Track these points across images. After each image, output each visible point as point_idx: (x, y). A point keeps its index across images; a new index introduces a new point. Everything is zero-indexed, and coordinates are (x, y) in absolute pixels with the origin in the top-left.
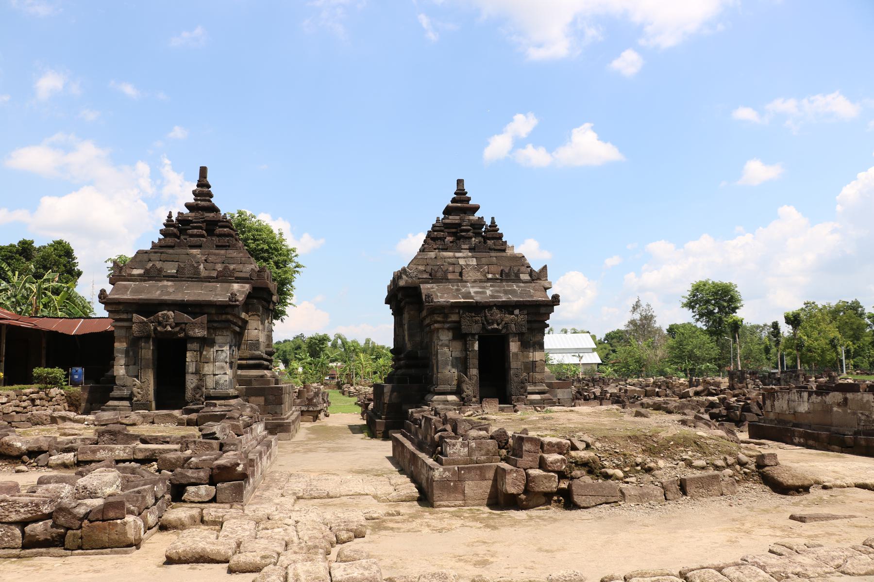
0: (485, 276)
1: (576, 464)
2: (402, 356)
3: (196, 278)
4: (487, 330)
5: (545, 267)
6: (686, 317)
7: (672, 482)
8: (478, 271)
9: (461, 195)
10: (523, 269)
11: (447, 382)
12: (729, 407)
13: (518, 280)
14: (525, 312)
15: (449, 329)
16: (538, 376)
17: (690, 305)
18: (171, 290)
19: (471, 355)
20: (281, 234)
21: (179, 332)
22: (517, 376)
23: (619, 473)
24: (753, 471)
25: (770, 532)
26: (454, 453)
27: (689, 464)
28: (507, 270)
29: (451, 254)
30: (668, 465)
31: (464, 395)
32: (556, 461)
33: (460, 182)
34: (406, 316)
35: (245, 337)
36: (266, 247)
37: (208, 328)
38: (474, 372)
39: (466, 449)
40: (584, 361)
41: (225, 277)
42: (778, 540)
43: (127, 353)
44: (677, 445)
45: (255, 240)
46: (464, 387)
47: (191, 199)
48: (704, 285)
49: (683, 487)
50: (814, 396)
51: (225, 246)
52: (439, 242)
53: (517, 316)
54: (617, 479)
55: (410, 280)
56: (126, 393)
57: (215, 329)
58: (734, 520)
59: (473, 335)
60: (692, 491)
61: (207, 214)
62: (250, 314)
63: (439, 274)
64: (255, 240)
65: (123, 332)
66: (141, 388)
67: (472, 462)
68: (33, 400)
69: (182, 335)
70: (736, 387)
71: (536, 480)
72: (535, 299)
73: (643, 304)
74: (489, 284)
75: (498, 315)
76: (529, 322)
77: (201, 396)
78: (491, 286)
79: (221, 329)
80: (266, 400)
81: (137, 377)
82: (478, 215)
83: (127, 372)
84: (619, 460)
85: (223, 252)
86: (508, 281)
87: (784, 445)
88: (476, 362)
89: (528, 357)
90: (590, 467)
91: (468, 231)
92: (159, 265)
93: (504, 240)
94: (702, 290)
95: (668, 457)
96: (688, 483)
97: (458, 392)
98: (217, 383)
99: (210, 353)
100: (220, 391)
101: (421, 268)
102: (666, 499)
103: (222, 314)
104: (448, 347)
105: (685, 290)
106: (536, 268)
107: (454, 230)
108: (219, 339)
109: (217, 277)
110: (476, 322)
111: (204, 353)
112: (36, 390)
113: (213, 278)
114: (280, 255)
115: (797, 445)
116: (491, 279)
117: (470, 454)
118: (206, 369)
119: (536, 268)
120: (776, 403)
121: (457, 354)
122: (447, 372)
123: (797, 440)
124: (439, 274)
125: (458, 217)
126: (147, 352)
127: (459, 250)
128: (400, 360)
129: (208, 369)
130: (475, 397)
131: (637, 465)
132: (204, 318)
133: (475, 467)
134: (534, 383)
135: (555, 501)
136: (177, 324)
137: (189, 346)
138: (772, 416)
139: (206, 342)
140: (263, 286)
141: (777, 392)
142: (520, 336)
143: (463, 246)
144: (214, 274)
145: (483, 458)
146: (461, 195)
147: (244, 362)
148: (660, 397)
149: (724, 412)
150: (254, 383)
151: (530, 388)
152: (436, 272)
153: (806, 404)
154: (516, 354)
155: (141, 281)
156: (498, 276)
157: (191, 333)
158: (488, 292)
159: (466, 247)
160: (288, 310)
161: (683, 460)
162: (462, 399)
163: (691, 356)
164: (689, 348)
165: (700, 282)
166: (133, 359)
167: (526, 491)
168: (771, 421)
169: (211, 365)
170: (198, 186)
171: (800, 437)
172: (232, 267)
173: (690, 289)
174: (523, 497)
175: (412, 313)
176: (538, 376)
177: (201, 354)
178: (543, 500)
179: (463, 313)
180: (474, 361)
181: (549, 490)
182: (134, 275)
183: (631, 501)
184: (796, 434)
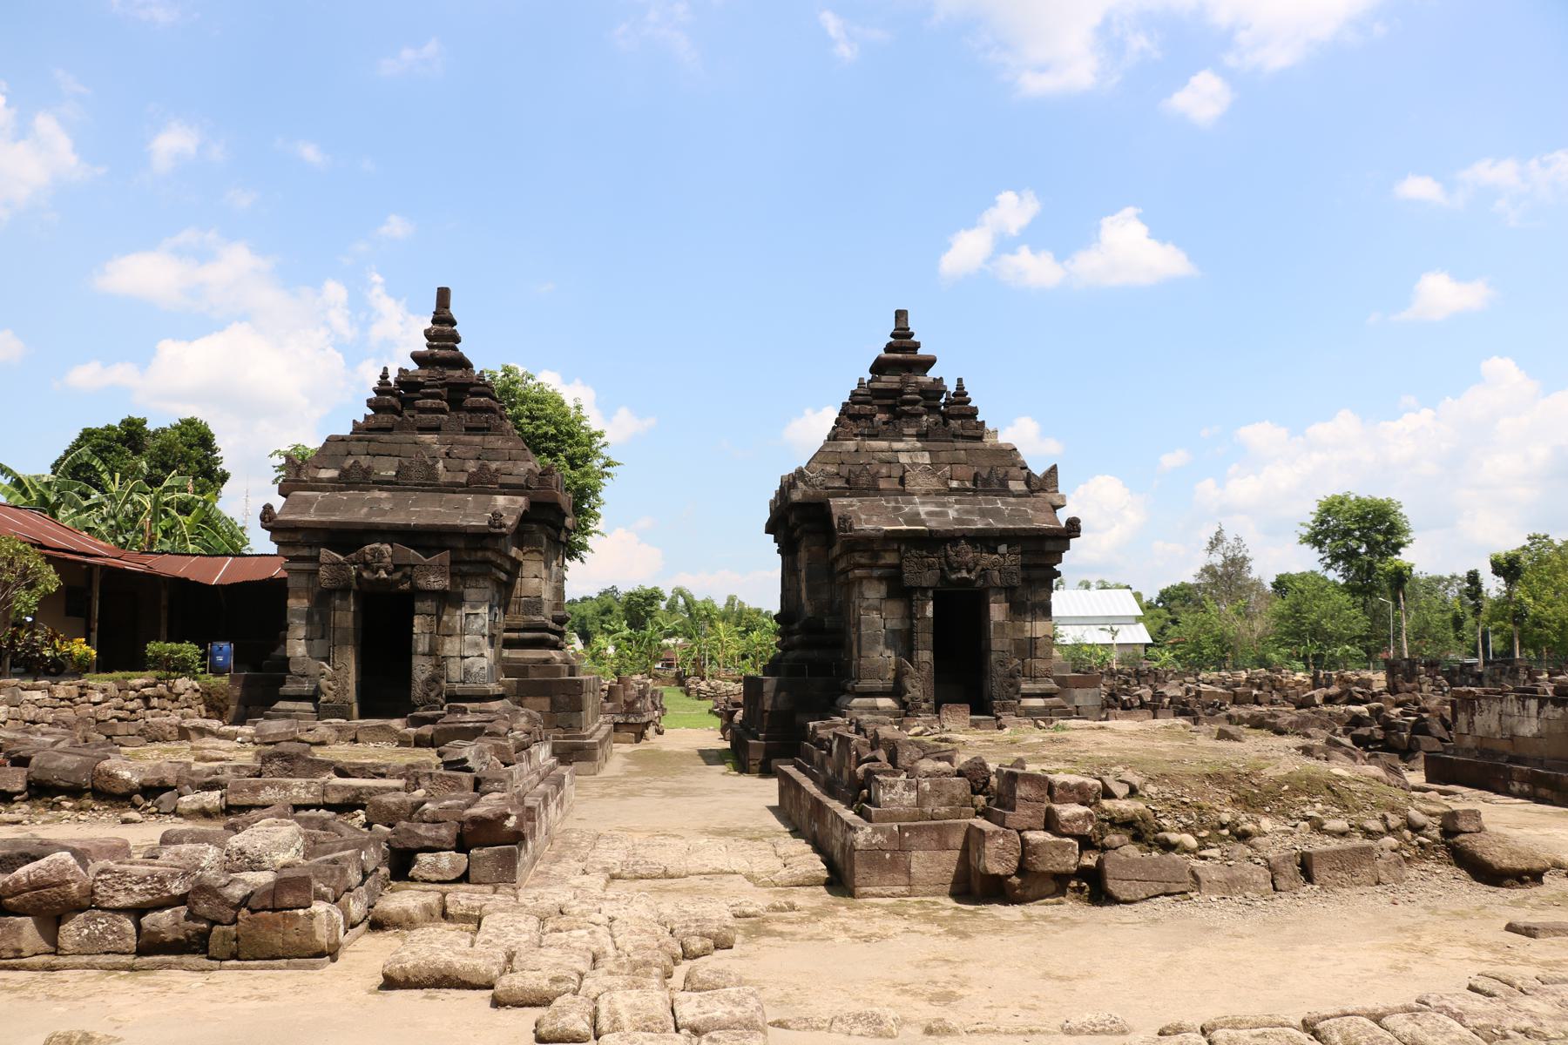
1: (1112, 822)
2: (796, 626)
3: (431, 485)
4: (951, 583)
5: (1054, 468)
6: (1307, 561)
7: (1287, 859)
8: (934, 474)
9: (902, 338)
10: (1014, 471)
11: (875, 673)
12: (1388, 725)
13: (1004, 491)
14: (1019, 549)
15: (880, 579)
16: (1040, 665)
17: (1315, 539)
18: (387, 507)
19: (919, 625)
20: (578, 408)
21: (400, 581)
22: (1002, 663)
23: (1190, 840)
24: (1436, 841)
25: (1468, 952)
26: (893, 800)
27: (1318, 827)
28: (985, 474)
29: (884, 444)
30: (1279, 827)
31: (907, 698)
32: (1076, 818)
33: (901, 315)
34: (803, 555)
35: (517, 592)
36: (552, 430)
37: (452, 575)
38: (925, 656)
39: (914, 794)
40: (1120, 639)
41: (482, 484)
42: (1485, 968)
43: (309, 617)
44: (1295, 791)
45: (533, 418)
46: (908, 683)
47: (422, 345)
48: (1342, 503)
49: (1306, 868)
50: (1550, 707)
51: (483, 429)
52: (863, 423)
53: (1003, 555)
54: (1187, 852)
55: (810, 491)
56: (307, 687)
57: (464, 576)
58: (1400, 929)
59: (924, 590)
60: (1323, 875)
61: (449, 373)
62: (526, 549)
63: (863, 481)
64: (533, 418)
65: (302, 581)
66: (333, 679)
67: (923, 816)
68: (146, 699)
69: (406, 586)
70: (1401, 687)
71: (1040, 852)
72: (1035, 525)
73: (1229, 537)
74: (952, 499)
75: (968, 554)
76: (1024, 566)
77: (440, 694)
78: (957, 502)
79: (475, 576)
80: (553, 703)
81: (327, 660)
82: (932, 373)
83: (309, 651)
84: (1189, 816)
85: (477, 439)
86: (986, 493)
87: (1491, 796)
88: (929, 638)
89: (1022, 631)
90: (1137, 829)
91: (914, 403)
92: (365, 461)
93: (979, 418)
94: (1337, 512)
95: (1279, 812)
96: (1315, 861)
97: (896, 692)
98: (467, 672)
99: (456, 618)
100: (471, 687)
101: (832, 469)
102: (1275, 889)
103: (476, 550)
105: (1307, 512)
106: (1038, 470)
107: (890, 402)
108: (471, 594)
109: (467, 484)
110: (930, 567)
111: (445, 618)
112: (152, 681)
113: (461, 485)
114: (577, 443)
115: (1516, 796)
116: (957, 489)
117: (920, 803)
118: (448, 646)
119: (1038, 470)
120: (1477, 718)
121: (894, 624)
122: (876, 656)
123: (1516, 787)
124: (863, 481)
125: (897, 379)
126: (345, 615)
127: (899, 437)
128: (792, 633)
129: (451, 647)
130: (926, 701)
131: (1223, 827)
132: (444, 557)
133: (930, 827)
134: (1033, 678)
135: (1074, 890)
136: (397, 567)
137: (418, 605)
138: (1469, 742)
139: (449, 599)
141: (1478, 698)
142: (1009, 591)
143: (907, 431)
144: (463, 479)
145: (943, 810)
146: (902, 338)
147: (514, 635)
148: (1260, 704)
149: (1379, 734)
150: (531, 671)
151: (1026, 686)
153: (1534, 722)
154: (1001, 625)
155: (334, 489)
156: (968, 484)
157: (422, 583)
158: (952, 514)
159: (912, 431)
160: (591, 541)
161: (1306, 819)
162: (904, 705)
163: (1317, 632)
164: (1313, 617)
165: (1334, 497)
166: (320, 629)
167: (1021, 871)
168: (1468, 751)
169: (456, 640)
170: (434, 322)
171: (1522, 782)
172: (494, 466)
173: (1315, 509)
174: (1015, 880)
175: (814, 549)
176: (1040, 665)
177: (439, 619)
178: (1052, 887)
180: (925, 637)
181: (1063, 869)
182: (321, 480)
183: (1211, 891)
184: (1515, 775)
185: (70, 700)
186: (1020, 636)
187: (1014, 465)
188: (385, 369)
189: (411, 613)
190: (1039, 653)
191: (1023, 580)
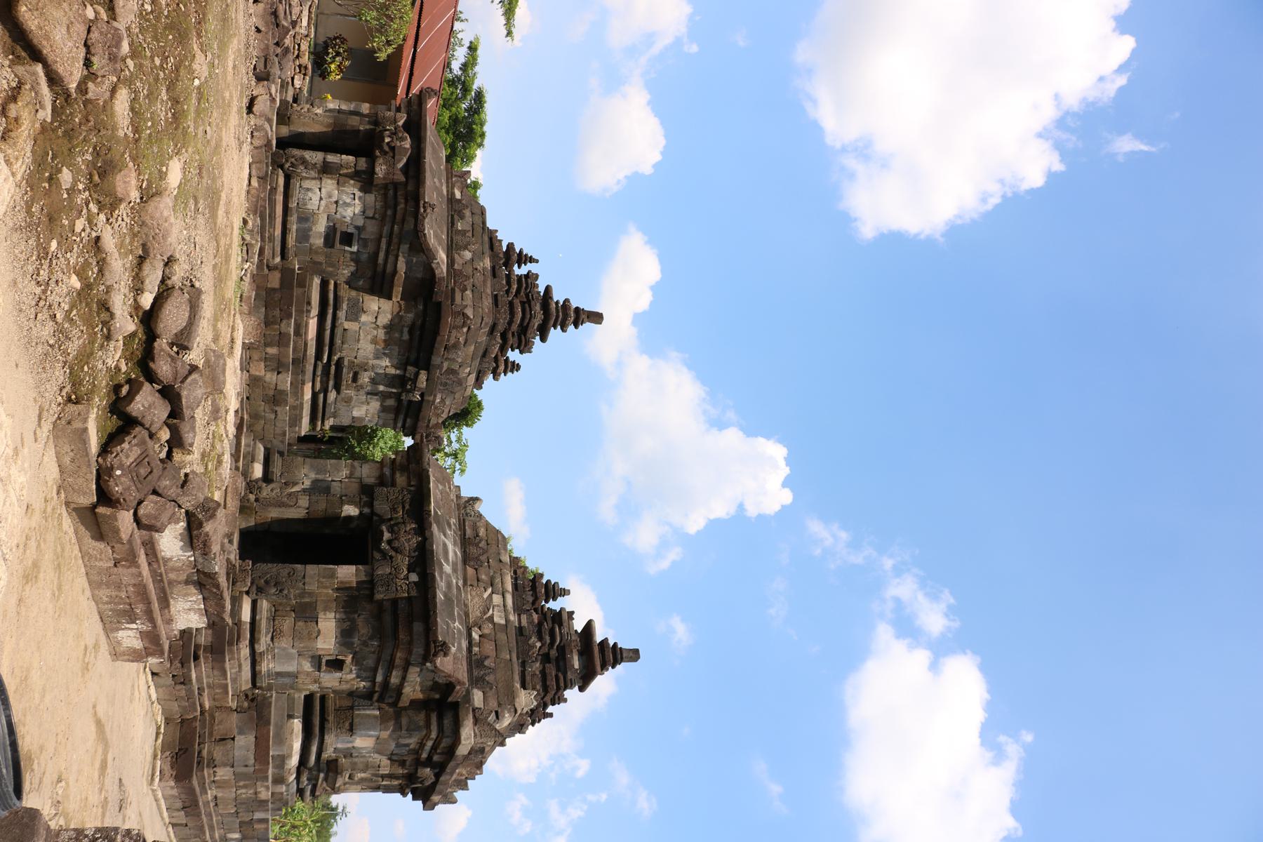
0: (475, 624)
9: (614, 656)
14: (414, 593)
16: (287, 623)
29: (509, 587)
33: (634, 655)
35: (367, 297)
47: (558, 296)
53: (407, 578)
57: (385, 195)
59: (371, 505)
62: (402, 303)
63: (473, 550)
75: (409, 542)
76: (395, 602)
80: (274, 289)
89: (326, 609)
100: (295, 183)
101: (482, 532)
104: (350, 476)
108: (371, 198)
110: (394, 510)
118: (329, 181)
121: (336, 488)
122: (304, 471)
124: (473, 550)
130: (257, 500)
136: (393, 149)
139: (366, 180)
140: (443, 313)
142: (368, 587)
146: (614, 656)
147: (332, 287)
150: (300, 290)
152: (477, 545)
154: (333, 575)
157: (381, 161)
159: (524, 622)
170: (577, 309)
179: (409, 492)
185: (298, 57)
186: (320, 607)
187: (500, 705)
188: (537, 261)
190: (300, 624)
191: (380, 602)
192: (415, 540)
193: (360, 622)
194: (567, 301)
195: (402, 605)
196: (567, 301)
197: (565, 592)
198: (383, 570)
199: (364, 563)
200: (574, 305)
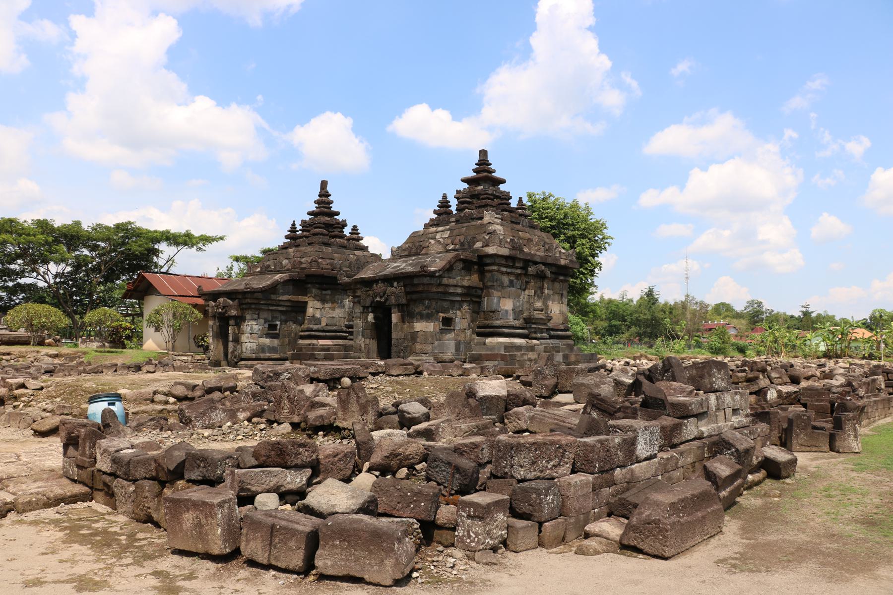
14: (402, 284)
35: (307, 314)
76: (407, 293)
89: (413, 327)
108: (248, 317)
110: (369, 296)
124: (414, 250)
136: (224, 307)
139: (240, 320)
142: (401, 307)
154: (396, 325)
189: (229, 325)
190: (418, 340)
192: (381, 284)
193: (417, 310)
194: (315, 202)
195: (408, 290)
196: (315, 202)
197: (445, 197)
198: (393, 300)
199: (390, 310)
200: (318, 198)
